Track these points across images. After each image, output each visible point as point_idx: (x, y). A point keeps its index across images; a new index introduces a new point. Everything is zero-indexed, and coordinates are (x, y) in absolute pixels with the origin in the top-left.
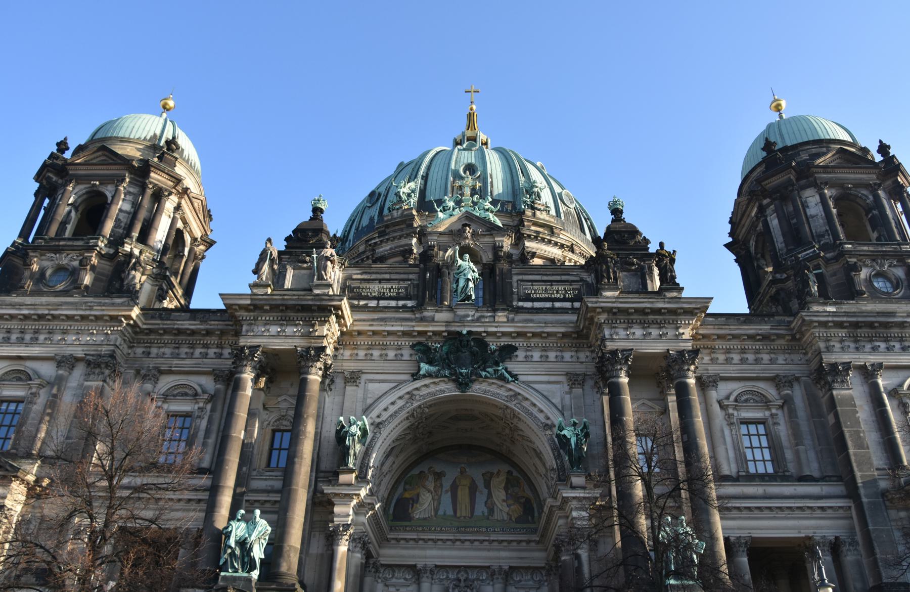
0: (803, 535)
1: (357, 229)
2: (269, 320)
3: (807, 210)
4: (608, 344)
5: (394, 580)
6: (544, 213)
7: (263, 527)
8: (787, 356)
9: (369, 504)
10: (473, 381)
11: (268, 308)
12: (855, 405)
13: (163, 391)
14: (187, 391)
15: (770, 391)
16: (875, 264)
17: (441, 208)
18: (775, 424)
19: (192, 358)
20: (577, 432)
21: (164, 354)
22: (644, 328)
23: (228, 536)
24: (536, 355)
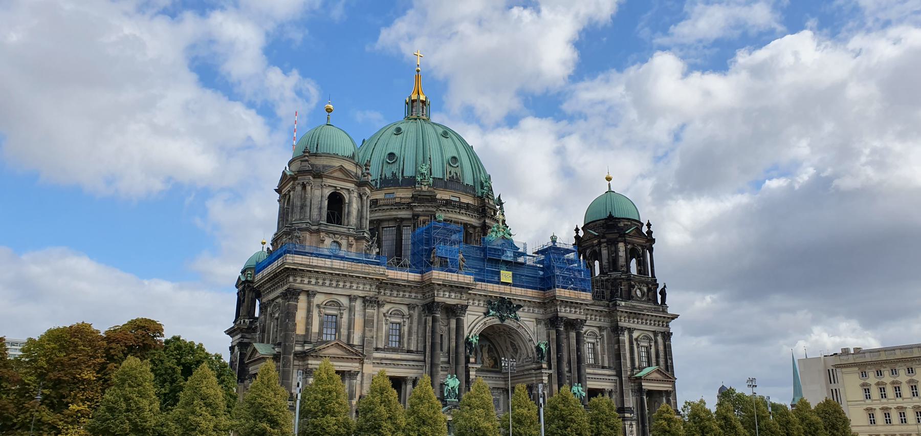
1: (381, 175)
13: (389, 313)
15: (597, 330)
18: (598, 345)
22: (570, 308)
24: (526, 309)
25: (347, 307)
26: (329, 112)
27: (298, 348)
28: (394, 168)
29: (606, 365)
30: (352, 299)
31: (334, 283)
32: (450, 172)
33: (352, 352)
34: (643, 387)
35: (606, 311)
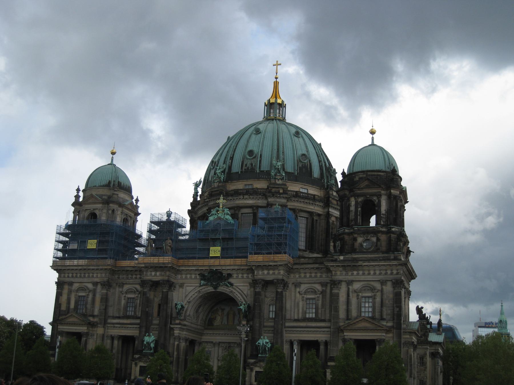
0: (316, 339)
1: (208, 181)
2: (151, 271)
3: (351, 207)
4: (255, 276)
5: (207, 346)
6: (280, 180)
7: (153, 338)
8: (326, 274)
9: (186, 328)
10: (219, 286)
11: (149, 267)
12: (338, 296)
13: (125, 291)
14: (133, 290)
15: (318, 287)
16: (364, 236)
17: (211, 214)
18: (318, 300)
19: (132, 279)
20: (245, 307)
21: (124, 278)
23: (144, 341)
24: (240, 275)
25: (91, 291)
26: (113, 155)
27: (61, 318)
28: (212, 172)
29: (327, 317)
30: (95, 284)
31: (82, 275)
32: (246, 165)
33: (81, 320)
34: (346, 337)
35: (324, 268)
